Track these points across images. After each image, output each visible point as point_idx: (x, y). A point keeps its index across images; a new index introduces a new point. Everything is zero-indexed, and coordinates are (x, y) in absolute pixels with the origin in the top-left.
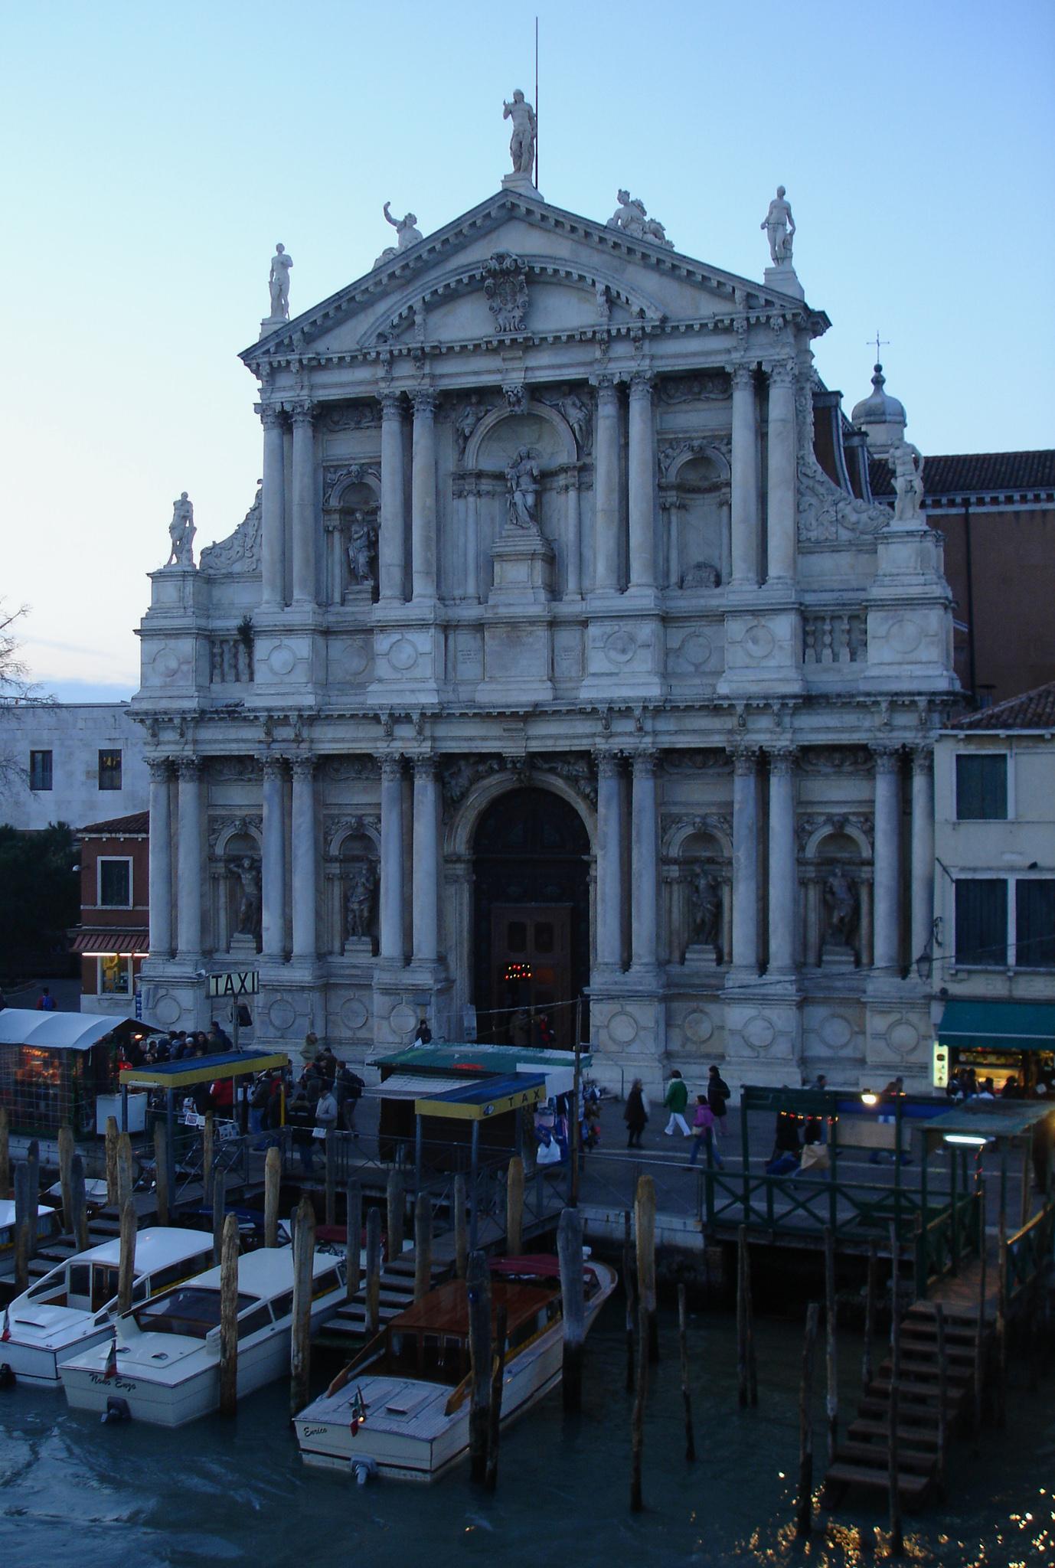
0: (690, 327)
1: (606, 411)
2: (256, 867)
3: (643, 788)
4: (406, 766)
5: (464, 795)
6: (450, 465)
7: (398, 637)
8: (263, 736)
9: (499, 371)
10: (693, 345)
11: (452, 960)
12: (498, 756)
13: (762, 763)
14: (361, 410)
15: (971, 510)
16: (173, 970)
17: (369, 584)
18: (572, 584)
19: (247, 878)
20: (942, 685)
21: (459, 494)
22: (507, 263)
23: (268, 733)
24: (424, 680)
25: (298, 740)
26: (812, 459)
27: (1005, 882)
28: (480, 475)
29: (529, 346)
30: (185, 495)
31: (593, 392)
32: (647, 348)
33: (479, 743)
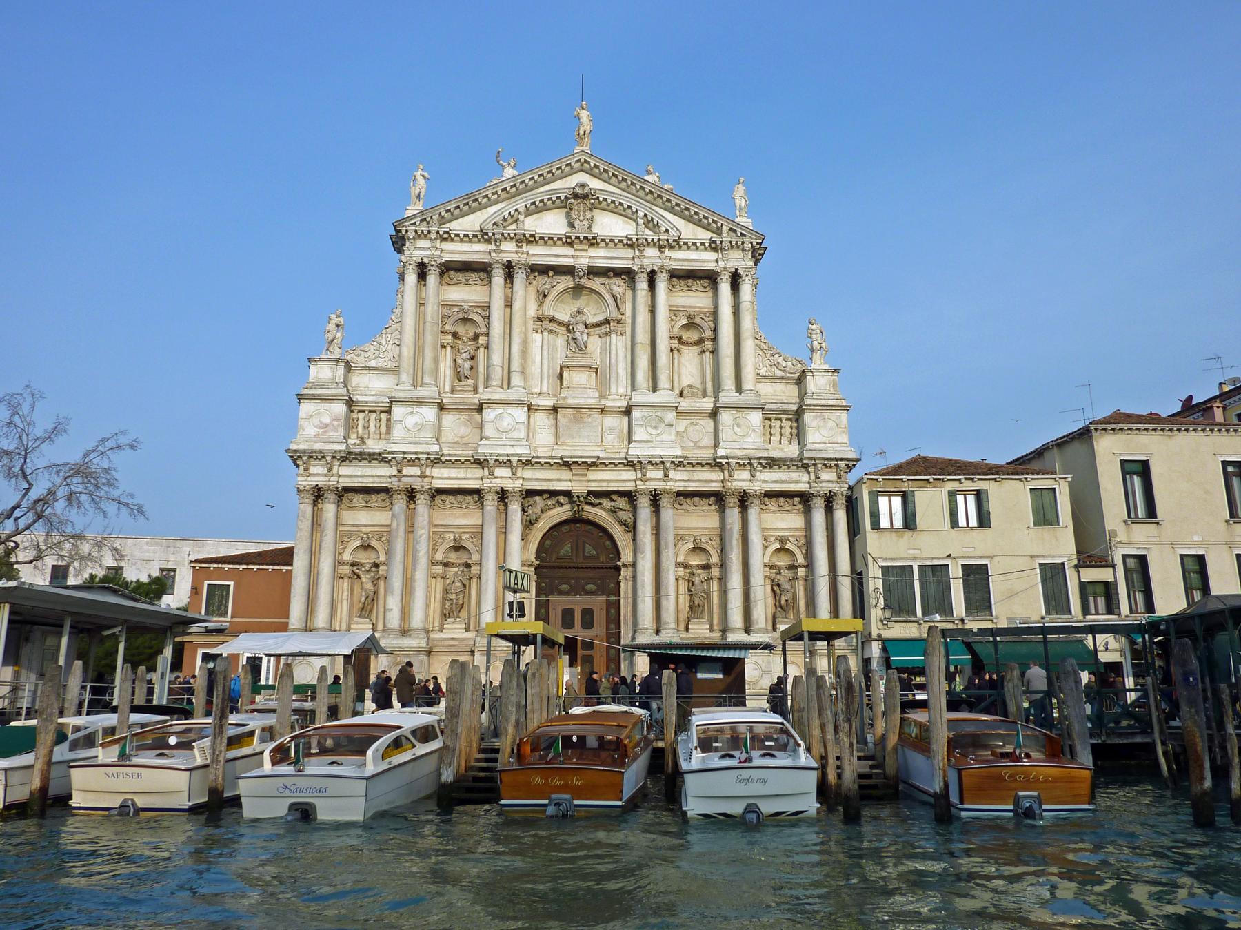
0: (694, 244)
4: (503, 496)
5: (537, 520)
6: (532, 311)
7: (499, 410)
8: (395, 473)
9: (572, 256)
10: (693, 255)
12: (567, 494)
13: (744, 500)
17: (470, 381)
19: (366, 578)
22: (586, 190)
23: (400, 471)
24: (521, 439)
25: (423, 475)
28: (552, 320)
29: (593, 242)
32: (667, 252)
33: (554, 483)
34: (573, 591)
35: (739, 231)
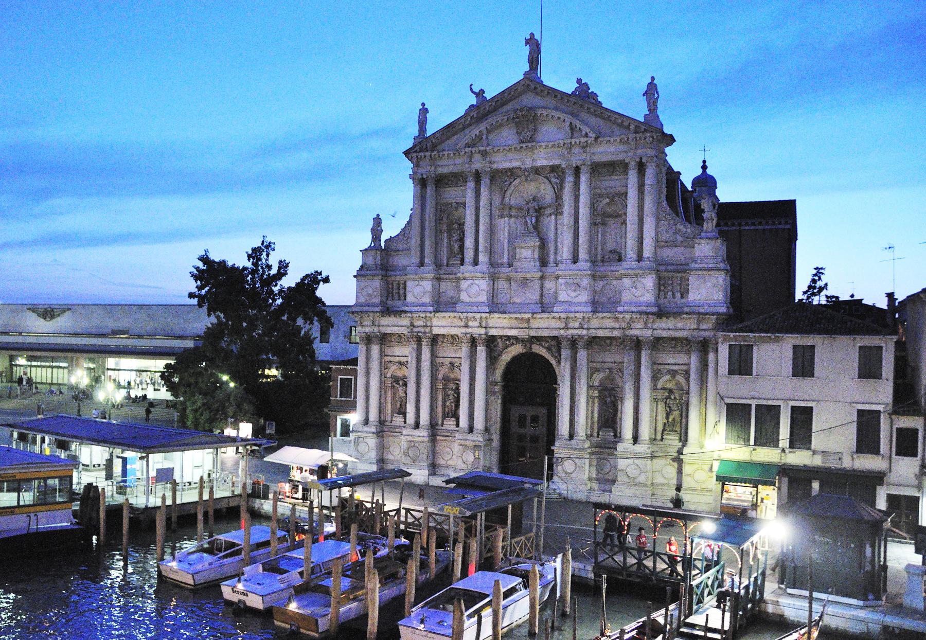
1: (569, 179)
2: (405, 385)
3: (582, 355)
5: (500, 355)
11: (492, 430)
12: (516, 338)
13: (637, 344)
14: (457, 178)
15: (742, 228)
16: (366, 429)
18: (552, 258)
20: (723, 310)
21: (502, 217)
26: (665, 202)
27: (750, 405)
30: (378, 215)
31: (564, 171)
34: (530, 402)
35: (643, 127)
